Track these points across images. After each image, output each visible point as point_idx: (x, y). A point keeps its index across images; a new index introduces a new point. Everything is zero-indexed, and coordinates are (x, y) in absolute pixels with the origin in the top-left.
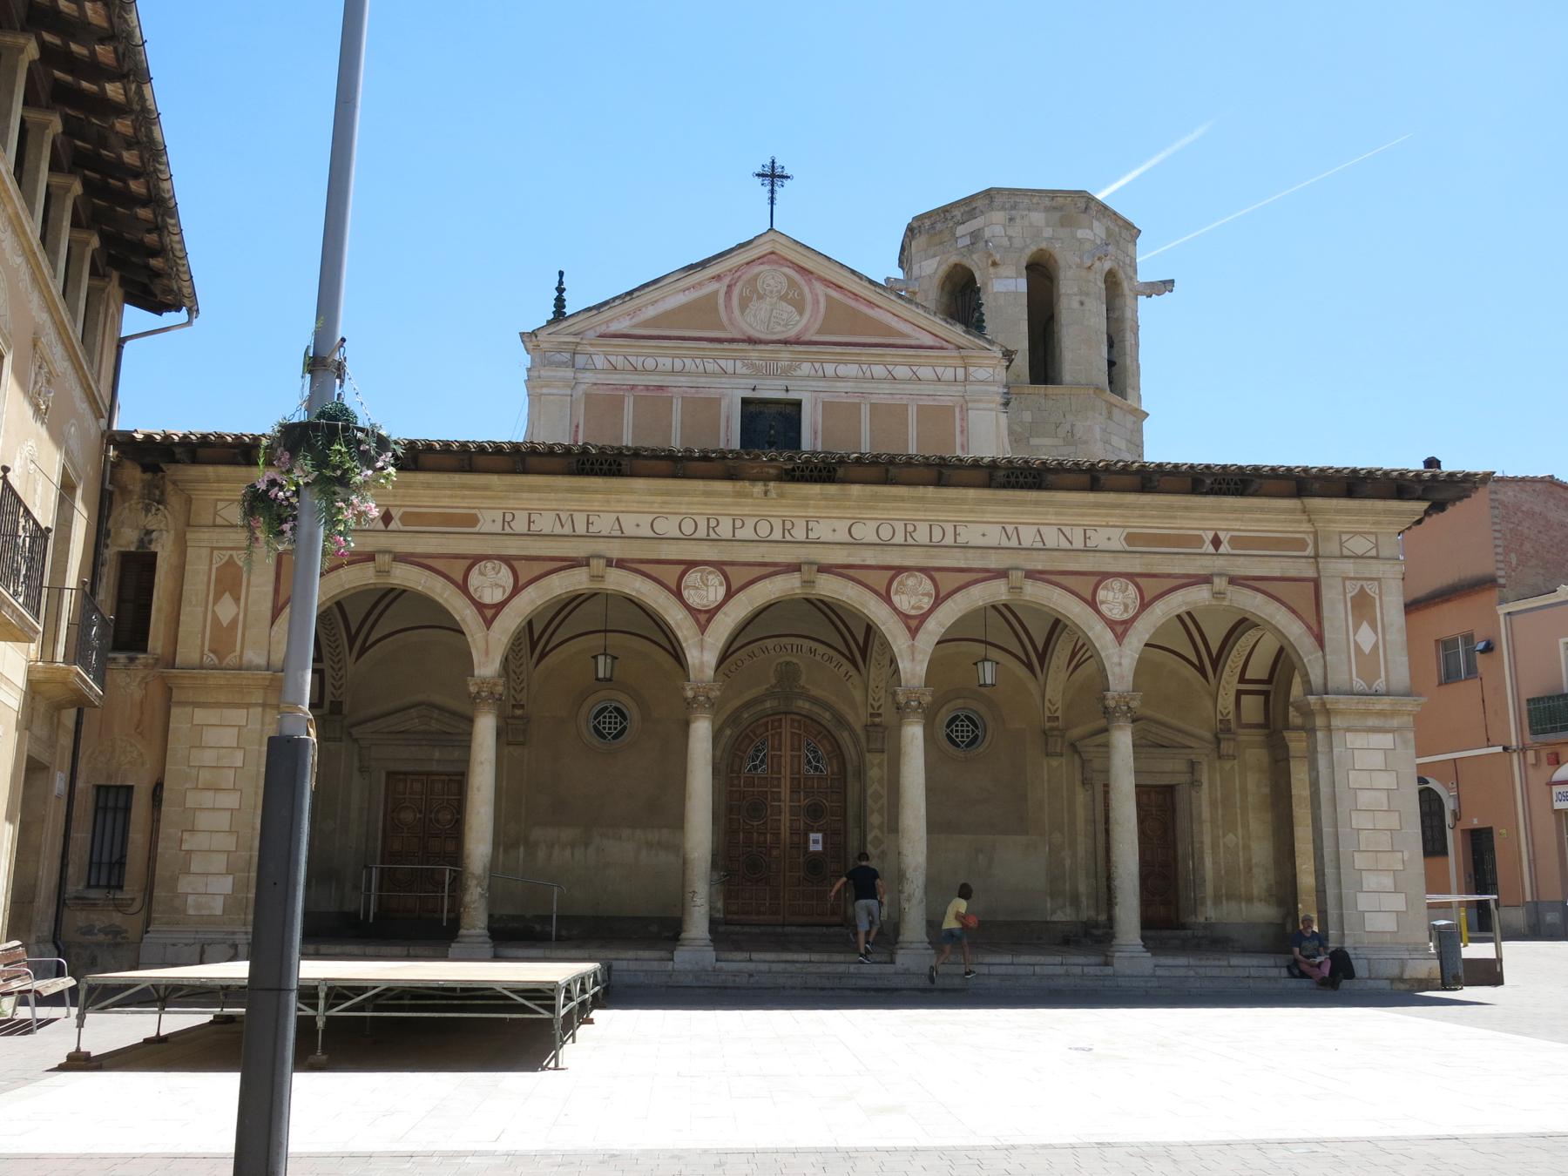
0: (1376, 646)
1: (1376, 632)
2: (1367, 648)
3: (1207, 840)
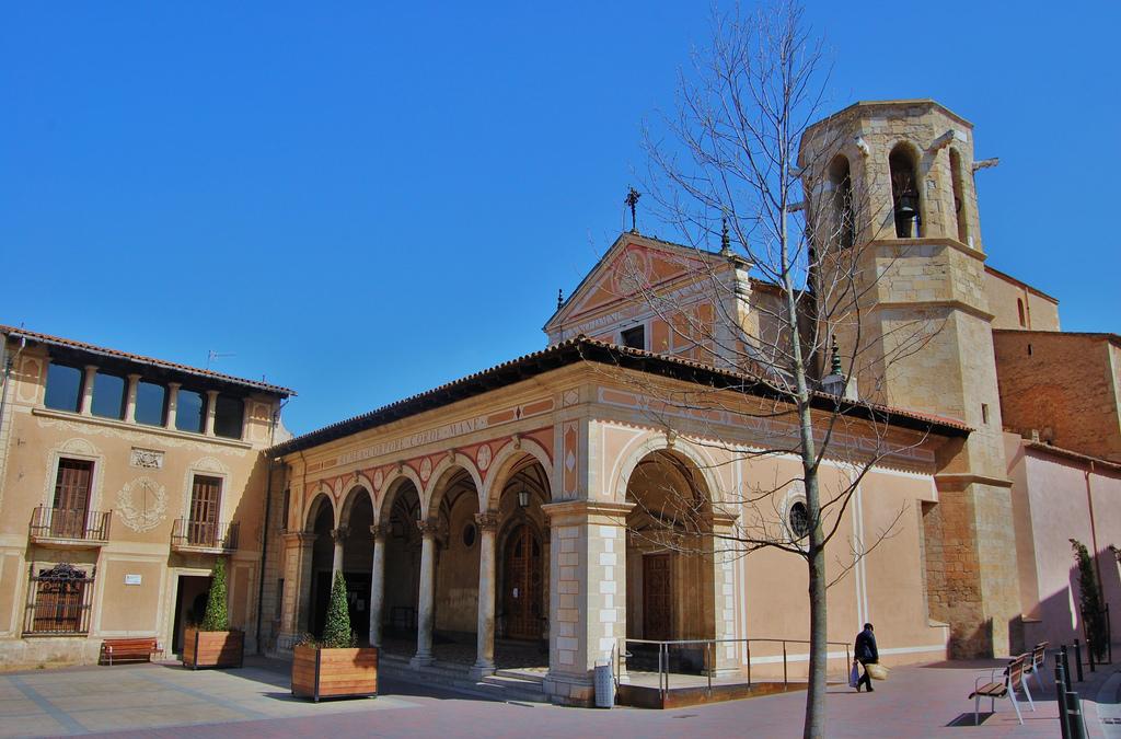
3: (681, 591)
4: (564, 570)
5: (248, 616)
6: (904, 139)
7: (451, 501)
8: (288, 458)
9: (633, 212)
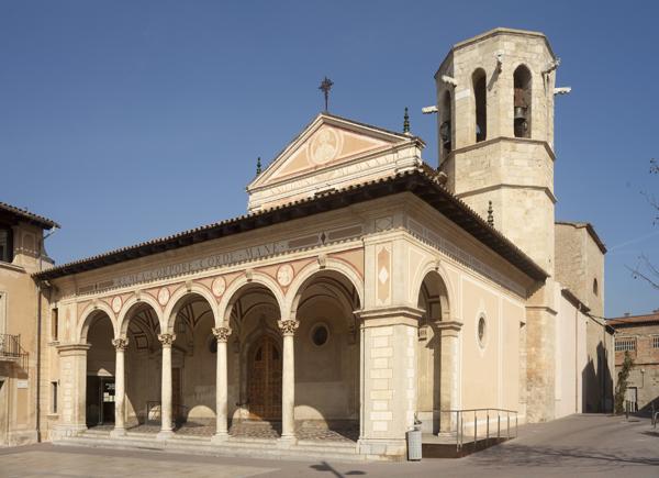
0: (388, 280)
1: (388, 271)
2: (383, 281)
4: (377, 361)
5: (29, 413)
7: (196, 318)
8: (57, 281)
9: (326, 98)
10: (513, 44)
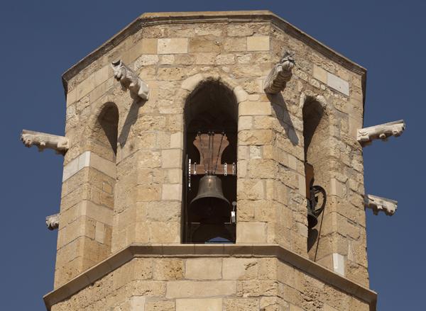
6: (216, 76)
10: (185, 42)
